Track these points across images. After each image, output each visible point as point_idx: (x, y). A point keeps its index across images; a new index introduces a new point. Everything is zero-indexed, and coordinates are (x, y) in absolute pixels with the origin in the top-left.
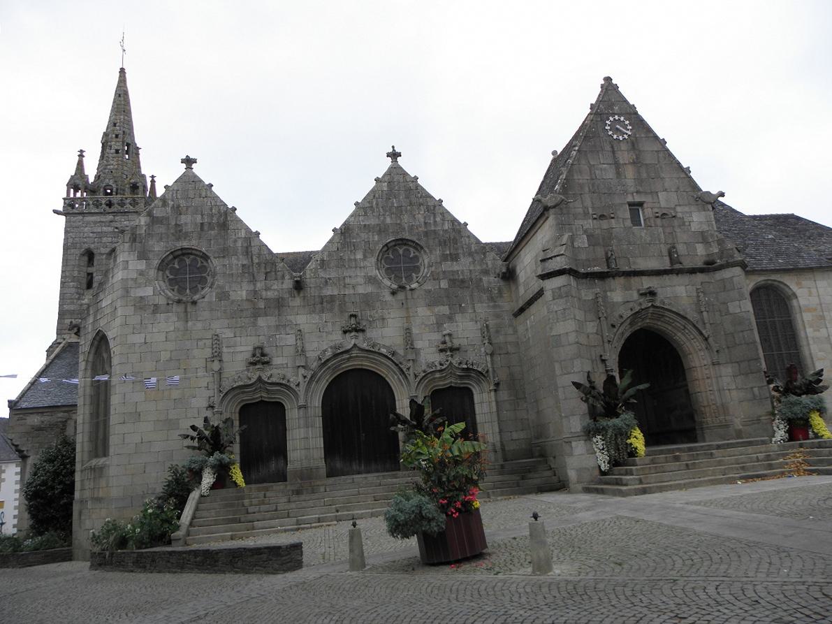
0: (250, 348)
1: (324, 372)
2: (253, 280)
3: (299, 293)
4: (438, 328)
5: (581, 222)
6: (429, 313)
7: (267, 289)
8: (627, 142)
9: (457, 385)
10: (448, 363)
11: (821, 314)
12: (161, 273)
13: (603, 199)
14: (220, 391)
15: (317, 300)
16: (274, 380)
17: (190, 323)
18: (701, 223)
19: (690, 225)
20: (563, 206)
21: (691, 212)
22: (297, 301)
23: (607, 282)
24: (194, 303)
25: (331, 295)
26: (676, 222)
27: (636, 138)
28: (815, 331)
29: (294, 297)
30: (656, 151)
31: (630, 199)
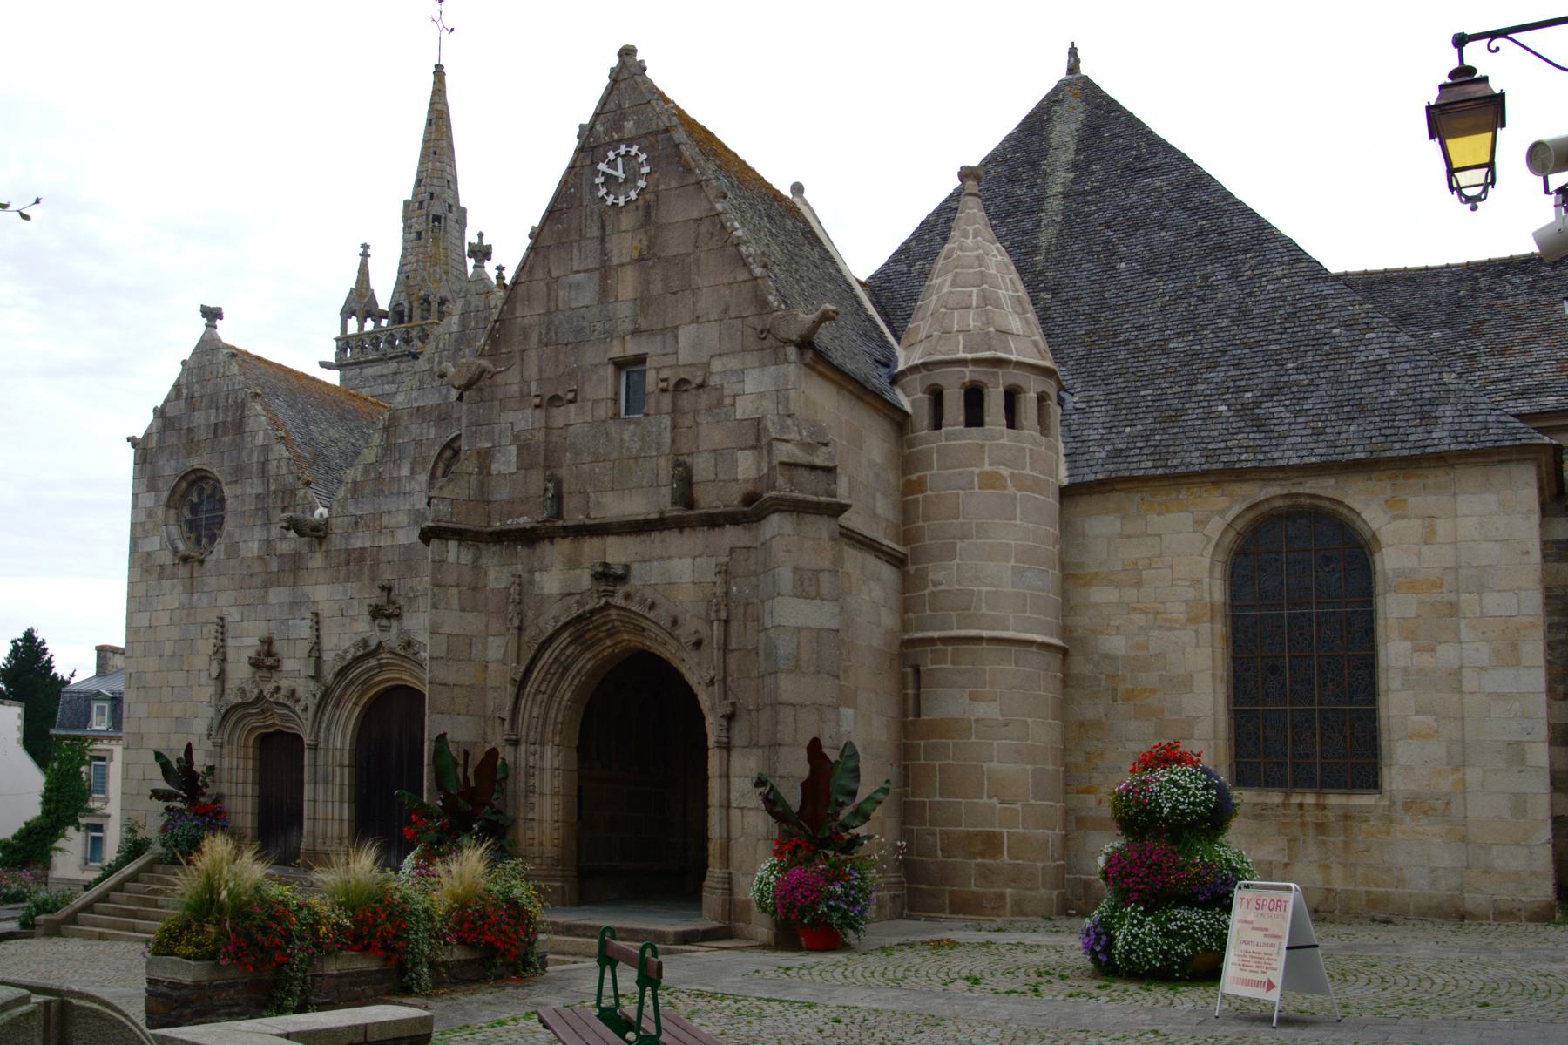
0: (255, 641)
2: (267, 524)
3: (320, 544)
5: (510, 416)
8: (637, 208)
11: (1453, 597)
12: (172, 512)
13: (562, 357)
15: (343, 557)
18: (762, 395)
19: (733, 405)
20: (484, 382)
21: (743, 371)
22: (317, 561)
23: (538, 550)
24: (202, 562)
25: (361, 549)
26: (704, 399)
27: (657, 193)
28: (1416, 650)
29: (315, 552)
30: (696, 220)
31: (616, 351)
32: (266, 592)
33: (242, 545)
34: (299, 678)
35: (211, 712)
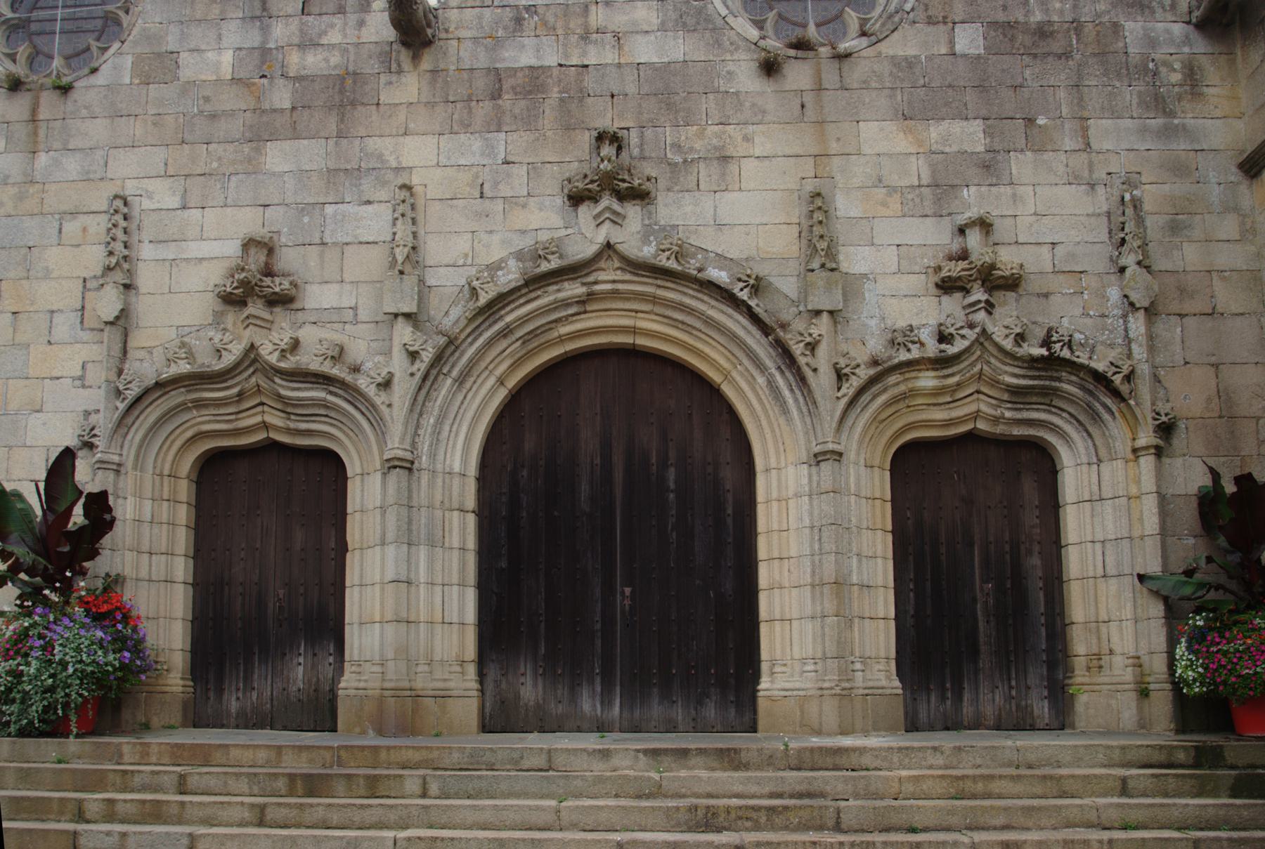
0: (232, 249)
1: (490, 343)
3: (416, 58)
4: (938, 200)
6: (902, 143)
7: (307, 43)
9: (1000, 429)
10: (971, 335)
14: (119, 393)
15: (481, 83)
16: (309, 360)
17: (43, 159)
24: (65, 90)
25: (531, 68)
29: (400, 72)
32: (258, 150)
33: (184, 57)
34: (356, 322)
35: (95, 398)
